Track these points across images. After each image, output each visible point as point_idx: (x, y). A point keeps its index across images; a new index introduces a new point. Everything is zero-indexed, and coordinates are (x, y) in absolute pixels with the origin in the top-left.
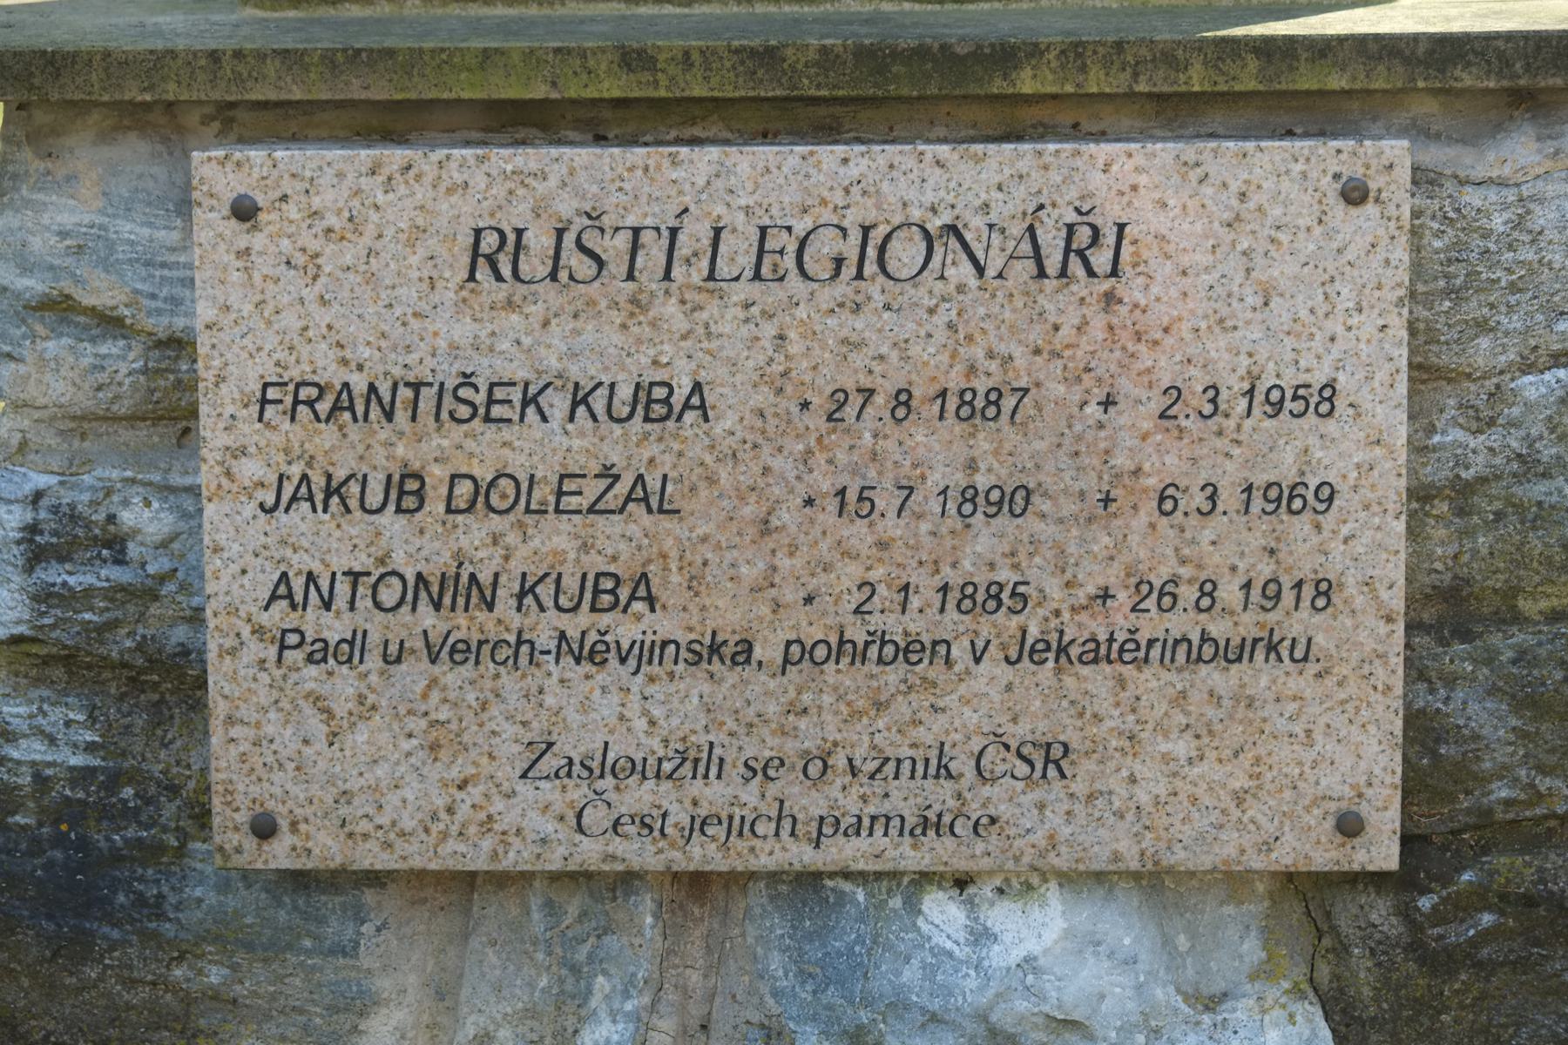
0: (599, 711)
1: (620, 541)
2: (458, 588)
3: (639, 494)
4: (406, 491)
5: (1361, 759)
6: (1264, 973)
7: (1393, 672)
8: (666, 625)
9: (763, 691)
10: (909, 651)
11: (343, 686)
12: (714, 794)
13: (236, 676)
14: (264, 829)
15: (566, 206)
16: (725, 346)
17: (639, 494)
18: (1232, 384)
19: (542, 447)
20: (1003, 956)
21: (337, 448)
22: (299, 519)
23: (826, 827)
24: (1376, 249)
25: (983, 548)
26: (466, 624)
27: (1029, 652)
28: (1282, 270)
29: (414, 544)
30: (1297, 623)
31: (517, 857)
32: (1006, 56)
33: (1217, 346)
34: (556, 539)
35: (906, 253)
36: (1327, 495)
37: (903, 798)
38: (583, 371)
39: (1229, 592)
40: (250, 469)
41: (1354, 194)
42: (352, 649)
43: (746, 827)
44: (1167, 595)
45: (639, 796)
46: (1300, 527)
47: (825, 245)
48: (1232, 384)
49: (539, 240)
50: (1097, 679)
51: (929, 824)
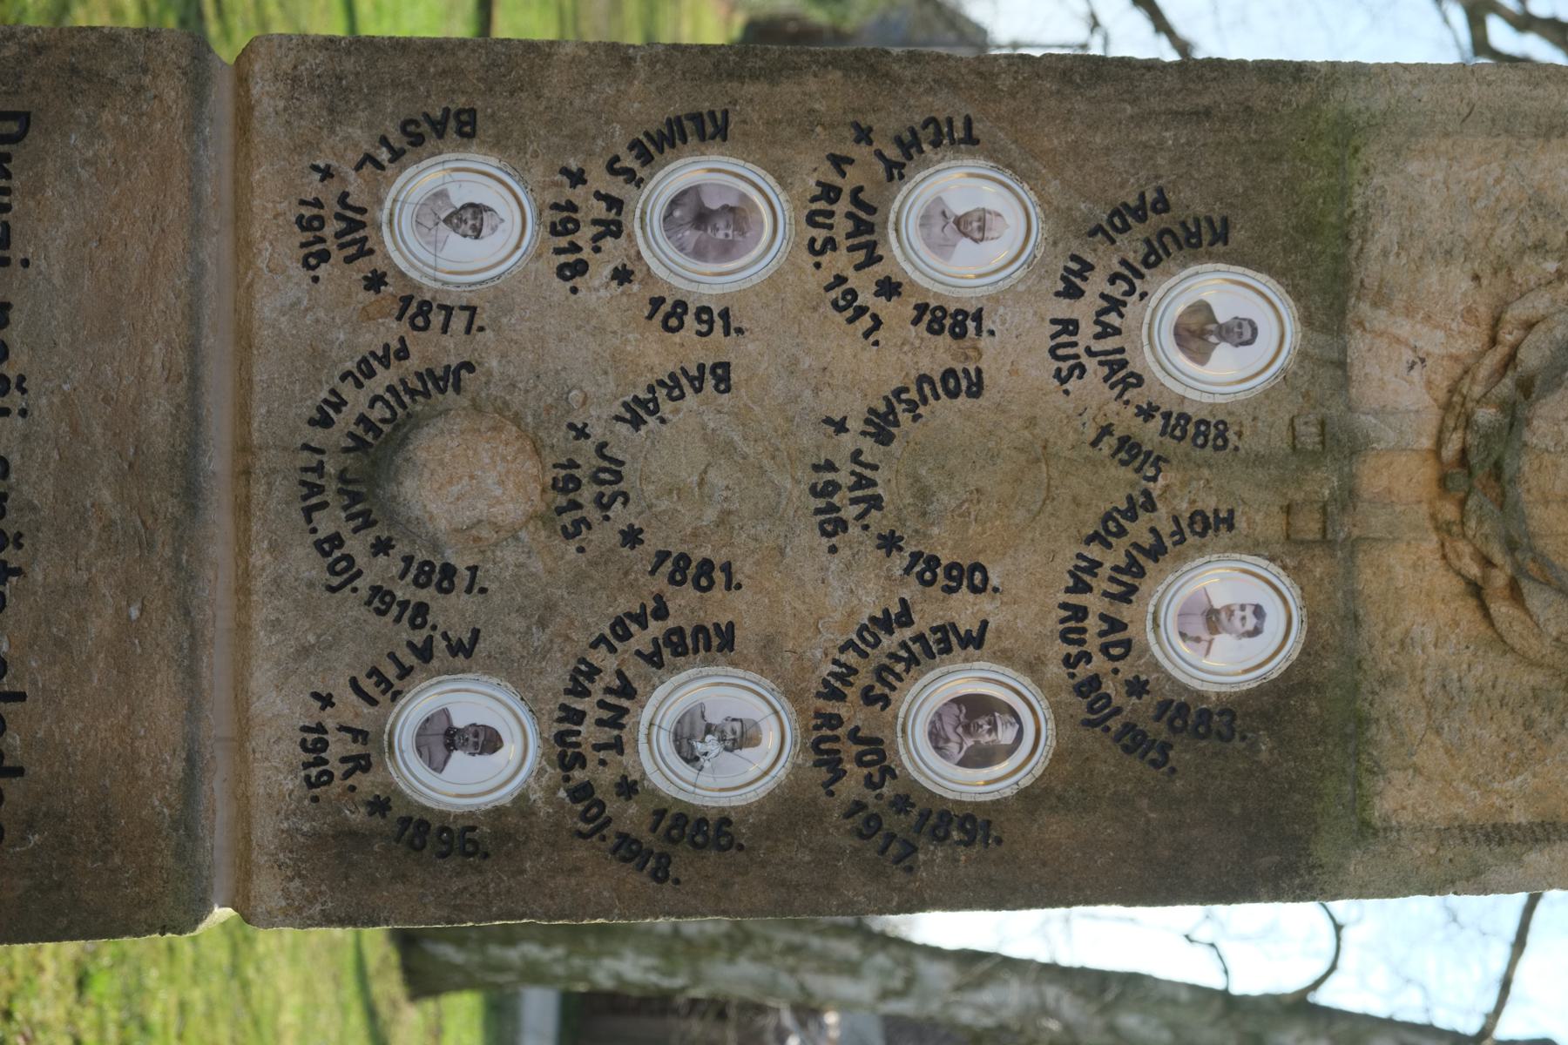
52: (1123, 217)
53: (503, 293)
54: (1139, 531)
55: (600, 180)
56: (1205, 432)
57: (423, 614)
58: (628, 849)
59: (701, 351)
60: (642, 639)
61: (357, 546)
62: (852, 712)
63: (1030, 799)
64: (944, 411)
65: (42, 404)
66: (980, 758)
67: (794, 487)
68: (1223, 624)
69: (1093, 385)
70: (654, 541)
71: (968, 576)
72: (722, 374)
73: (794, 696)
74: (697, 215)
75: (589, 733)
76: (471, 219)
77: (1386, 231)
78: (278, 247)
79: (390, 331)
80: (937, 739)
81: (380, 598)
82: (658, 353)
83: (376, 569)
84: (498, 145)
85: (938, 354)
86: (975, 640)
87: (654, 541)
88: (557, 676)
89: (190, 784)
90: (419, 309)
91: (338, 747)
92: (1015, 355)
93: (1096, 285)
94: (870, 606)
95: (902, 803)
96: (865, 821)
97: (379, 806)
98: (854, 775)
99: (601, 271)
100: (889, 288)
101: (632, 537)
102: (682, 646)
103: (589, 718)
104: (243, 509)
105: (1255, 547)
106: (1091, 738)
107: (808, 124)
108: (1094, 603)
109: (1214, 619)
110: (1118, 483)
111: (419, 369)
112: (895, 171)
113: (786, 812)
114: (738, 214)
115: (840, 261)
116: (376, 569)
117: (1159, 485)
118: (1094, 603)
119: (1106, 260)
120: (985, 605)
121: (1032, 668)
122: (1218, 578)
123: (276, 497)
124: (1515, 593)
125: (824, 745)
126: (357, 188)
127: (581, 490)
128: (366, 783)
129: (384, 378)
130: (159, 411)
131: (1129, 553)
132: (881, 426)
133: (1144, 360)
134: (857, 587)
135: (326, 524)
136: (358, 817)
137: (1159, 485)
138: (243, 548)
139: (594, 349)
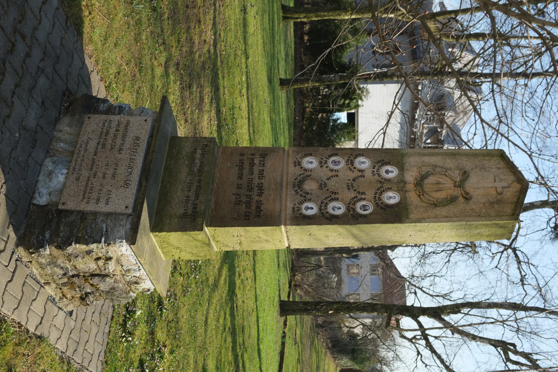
0: (92, 144)
1: (109, 146)
2: (107, 133)
3: (112, 148)
4: (117, 130)
5: (70, 206)
6: (51, 200)
7: (78, 209)
8: (99, 149)
9: (91, 157)
10: (92, 168)
11: (100, 125)
12: (82, 152)
13: (104, 117)
14: (89, 118)
15: (141, 144)
16: (125, 155)
17: (112, 148)
18: (110, 196)
19: (119, 141)
20: (59, 175)
21: (122, 127)
22: (117, 122)
23: (76, 160)
24: (121, 209)
25: (100, 175)
26: (104, 134)
27: (89, 178)
28: (121, 201)
29: (112, 131)
30: (85, 201)
31: (81, 136)
32: (147, 181)
33: (114, 195)
34: (110, 141)
35: (130, 170)
36: (97, 204)
37: (77, 167)
38: (125, 145)
39: (90, 195)
40: (122, 119)
41: (127, 207)
42: (104, 125)
43: (78, 154)
44: (91, 190)
45: (84, 146)
46: (95, 201)
47: (132, 164)
48: (110, 196)
49: (138, 142)
50: (85, 183)
51: (74, 169)
52: (379, 162)
53: (314, 169)
54: (382, 189)
55: (324, 159)
56: (389, 180)
57: (306, 197)
58: (327, 218)
59: (335, 174)
60: (329, 199)
61: (299, 191)
62: (351, 206)
63: (370, 214)
64: (361, 179)
65: (267, 178)
66: (364, 210)
67: (345, 186)
68: (392, 198)
69: (376, 176)
70: (330, 190)
71: (364, 193)
72: (337, 176)
73: (345, 204)
74: (334, 162)
75: (323, 208)
76: (311, 163)
77: (407, 164)
78: (291, 165)
79: (303, 172)
80: (360, 209)
81: (301, 195)
82: (330, 174)
83: (301, 193)
84: (314, 156)
85: (360, 174)
86: (364, 199)
87: (330, 190)
88: (320, 202)
89: (280, 212)
90: (306, 170)
91: (296, 209)
92: (368, 174)
93: (376, 168)
94: (353, 196)
95: (357, 214)
96: (353, 216)
97: (300, 214)
98: (351, 212)
99: (325, 167)
100: (355, 168)
101: (328, 190)
102: (333, 200)
103: (323, 206)
104: (287, 188)
105: (394, 191)
106: (377, 208)
107: (346, 154)
108: (377, 196)
109: (390, 198)
110: (379, 185)
111: (306, 175)
112: (355, 158)
113: (344, 215)
114: (339, 162)
115: (350, 166)
116: (301, 193)
117: (384, 185)
118: (377, 196)
119: (377, 165)
120: (365, 196)
121: (371, 202)
122: (390, 194)
123: (290, 187)
124: (423, 195)
125: (348, 209)
126: (300, 160)
127: (322, 186)
128: (299, 212)
129: (302, 176)
130: (279, 179)
131: (381, 191)
132: (354, 180)
133: (382, 174)
134: (351, 194)
135: (295, 189)
136: (298, 215)
137: (384, 185)
138: (287, 191)
139: (324, 173)
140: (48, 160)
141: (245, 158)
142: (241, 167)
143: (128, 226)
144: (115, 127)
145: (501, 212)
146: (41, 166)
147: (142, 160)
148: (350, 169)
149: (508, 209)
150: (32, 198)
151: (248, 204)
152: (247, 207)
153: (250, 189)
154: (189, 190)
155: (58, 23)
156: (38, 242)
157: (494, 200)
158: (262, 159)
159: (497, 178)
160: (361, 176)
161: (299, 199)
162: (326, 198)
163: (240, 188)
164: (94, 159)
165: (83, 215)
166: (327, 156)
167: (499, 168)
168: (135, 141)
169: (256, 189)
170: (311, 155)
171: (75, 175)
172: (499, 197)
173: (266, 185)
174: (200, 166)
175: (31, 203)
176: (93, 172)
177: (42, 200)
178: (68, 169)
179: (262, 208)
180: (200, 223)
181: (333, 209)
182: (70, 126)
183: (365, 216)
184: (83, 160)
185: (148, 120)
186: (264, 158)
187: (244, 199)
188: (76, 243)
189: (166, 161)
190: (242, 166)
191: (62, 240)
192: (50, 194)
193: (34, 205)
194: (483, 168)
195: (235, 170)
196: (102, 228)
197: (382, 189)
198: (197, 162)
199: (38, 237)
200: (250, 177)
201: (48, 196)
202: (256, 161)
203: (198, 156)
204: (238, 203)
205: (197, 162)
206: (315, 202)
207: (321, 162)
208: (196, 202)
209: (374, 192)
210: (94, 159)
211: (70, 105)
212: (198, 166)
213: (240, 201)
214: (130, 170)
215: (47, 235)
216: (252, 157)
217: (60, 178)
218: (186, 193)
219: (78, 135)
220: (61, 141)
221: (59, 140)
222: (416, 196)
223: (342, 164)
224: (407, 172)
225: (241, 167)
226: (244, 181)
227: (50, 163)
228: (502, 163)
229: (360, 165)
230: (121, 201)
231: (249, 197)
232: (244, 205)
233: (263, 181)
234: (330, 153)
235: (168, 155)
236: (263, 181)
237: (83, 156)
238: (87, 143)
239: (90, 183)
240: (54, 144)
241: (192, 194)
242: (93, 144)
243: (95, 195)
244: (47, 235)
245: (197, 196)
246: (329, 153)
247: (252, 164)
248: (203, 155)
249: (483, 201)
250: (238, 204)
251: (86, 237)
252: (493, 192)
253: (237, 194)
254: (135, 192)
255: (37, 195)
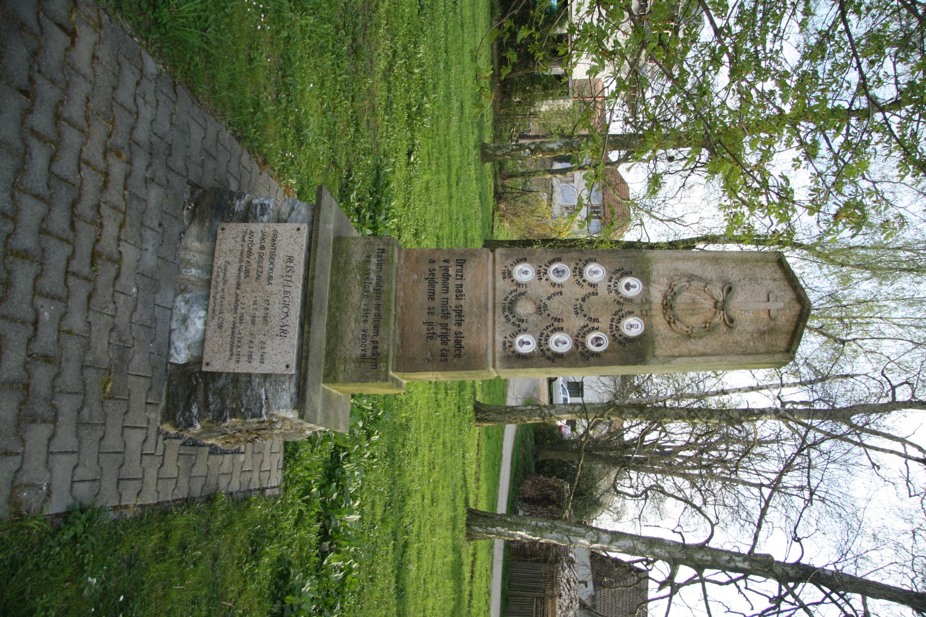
0: (232, 271)
1: (253, 273)
2: (250, 253)
3: (259, 276)
4: (262, 248)
5: (216, 366)
6: (192, 355)
7: (227, 370)
8: (242, 278)
9: (233, 291)
10: (236, 309)
11: (239, 239)
12: (221, 284)
13: (242, 226)
14: (223, 229)
15: (295, 268)
16: (276, 287)
17: (259, 276)
18: (265, 350)
19: (266, 265)
20: (197, 320)
21: (268, 240)
22: (260, 235)
23: (215, 298)
24: (280, 369)
25: (248, 318)
26: (245, 254)
27: (234, 323)
28: (279, 357)
29: (256, 249)
30: (234, 358)
31: (216, 260)
32: (309, 324)
33: (270, 348)
34: (255, 266)
35: (285, 310)
36: (250, 362)
37: (218, 308)
38: (275, 270)
39: (239, 350)
40: (267, 229)
41: (287, 366)
42: (243, 240)
43: (216, 288)
44: (239, 342)
45: (221, 275)
46: (246, 359)
47: (287, 299)
48: (265, 350)
49: (291, 265)
50: (230, 332)
51: (214, 311)
52: (617, 271)
53: (530, 282)
54: (620, 314)
55: (544, 267)
56: (630, 300)
57: (520, 326)
58: (548, 358)
59: (558, 290)
60: (550, 329)
61: (510, 317)
62: (580, 339)
63: (605, 351)
64: (592, 297)
65: (467, 298)
66: (599, 345)
67: (571, 308)
68: (633, 327)
69: (613, 294)
70: (552, 316)
71: (596, 320)
72: (561, 293)
73: (571, 336)
74: (557, 271)
75: (543, 342)
76: (526, 272)
77: (655, 273)
78: (499, 277)
79: (515, 287)
80: (592, 343)
81: (514, 324)
82: (552, 290)
83: (513, 320)
84: (530, 262)
85: (591, 290)
86: (597, 329)
87: (552, 316)
88: (538, 334)
89: (487, 349)
90: (519, 285)
91: (508, 344)
92: (602, 290)
93: (613, 280)
94: (582, 325)
95: (587, 352)
96: (582, 354)
97: (513, 352)
98: (580, 349)
99: (544, 279)
100: (584, 281)
101: (549, 315)
102: (556, 330)
103: (542, 340)
104: (494, 312)
105: (637, 316)
106: (614, 343)
107: (572, 259)
108: (614, 324)
109: (631, 326)
110: (617, 307)
111: (519, 292)
112: (585, 265)
113: (570, 353)
114: (563, 271)
115: (577, 277)
116: (513, 320)
117: (622, 309)
118: (614, 324)
119: (615, 277)
120: (599, 324)
121: (605, 333)
122: (631, 320)
123: (499, 310)
124: (674, 323)
125: (576, 344)
126: (510, 268)
127: (541, 309)
128: (512, 349)
129: (514, 294)
130: (483, 299)
131: (619, 316)
132: (584, 300)
133: (620, 290)
134: (580, 322)
135: (506, 314)
136: (510, 354)
137: (622, 309)
138: (494, 317)
139: (542, 290)
140: (180, 298)
141: (436, 266)
142: (432, 282)
143: (293, 390)
144: (259, 242)
145: (772, 346)
146: (171, 309)
147: (300, 293)
148: (579, 283)
149: (782, 343)
150: (169, 355)
151: (444, 337)
152: (444, 343)
153: (446, 315)
154: (365, 321)
155: (164, 97)
156: (185, 420)
157: (766, 328)
158: (459, 268)
159: (771, 296)
160: (593, 294)
161: (511, 329)
162: (547, 328)
163: (433, 314)
164: (237, 295)
165: (235, 378)
166: (546, 261)
167: (775, 280)
168: (288, 264)
169: (453, 314)
170: (525, 260)
171: (216, 320)
172: (772, 324)
173: (466, 309)
174: (378, 284)
175: (168, 362)
176: (239, 314)
177: (181, 356)
178: (207, 310)
179: (463, 343)
180: (383, 369)
181: (556, 344)
182: (200, 240)
183: (597, 355)
184: (223, 297)
185: (302, 228)
186: (462, 266)
187: (438, 330)
188: (231, 417)
189: (332, 276)
190: (433, 279)
191: (214, 415)
192: (189, 348)
193: (172, 364)
194: (753, 279)
195: (424, 286)
196: (260, 395)
197: (620, 314)
198: (373, 276)
199: (183, 414)
200: (445, 296)
201: (187, 351)
202: (452, 272)
203: (373, 267)
204: (431, 336)
205: (373, 276)
206: (531, 333)
207: (538, 273)
208: (377, 339)
209: (610, 317)
210: (237, 295)
211: (196, 205)
212: (374, 282)
213: (434, 333)
214: (285, 310)
215: (195, 410)
216: (446, 264)
217: (197, 324)
218: (362, 324)
219: (212, 254)
220: (192, 265)
221: (189, 264)
222: (665, 322)
223: (567, 277)
224: (654, 285)
225: (432, 282)
226: (437, 303)
227: (183, 303)
228: (779, 271)
229: (592, 276)
230: (279, 357)
231: (445, 326)
232: (439, 339)
233: (462, 302)
234: (551, 258)
235: (333, 266)
236: (462, 302)
237: (223, 290)
238: (226, 270)
239: (236, 331)
240: (183, 271)
241: (369, 326)
242: (233, 271)
243: (245, 350)
244: (195, 410)
245: (376, 328)
246: (550, 257)
247: (446, 276)
248: (379, 265)
249: (749, 329)
250: (431, 338)
251: (243, 410)
252: (764, 315)
253: (429, 323)
254: (295, 342)
255: (173, 351)
